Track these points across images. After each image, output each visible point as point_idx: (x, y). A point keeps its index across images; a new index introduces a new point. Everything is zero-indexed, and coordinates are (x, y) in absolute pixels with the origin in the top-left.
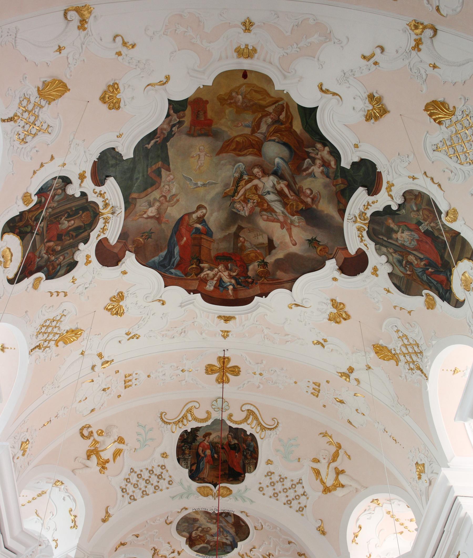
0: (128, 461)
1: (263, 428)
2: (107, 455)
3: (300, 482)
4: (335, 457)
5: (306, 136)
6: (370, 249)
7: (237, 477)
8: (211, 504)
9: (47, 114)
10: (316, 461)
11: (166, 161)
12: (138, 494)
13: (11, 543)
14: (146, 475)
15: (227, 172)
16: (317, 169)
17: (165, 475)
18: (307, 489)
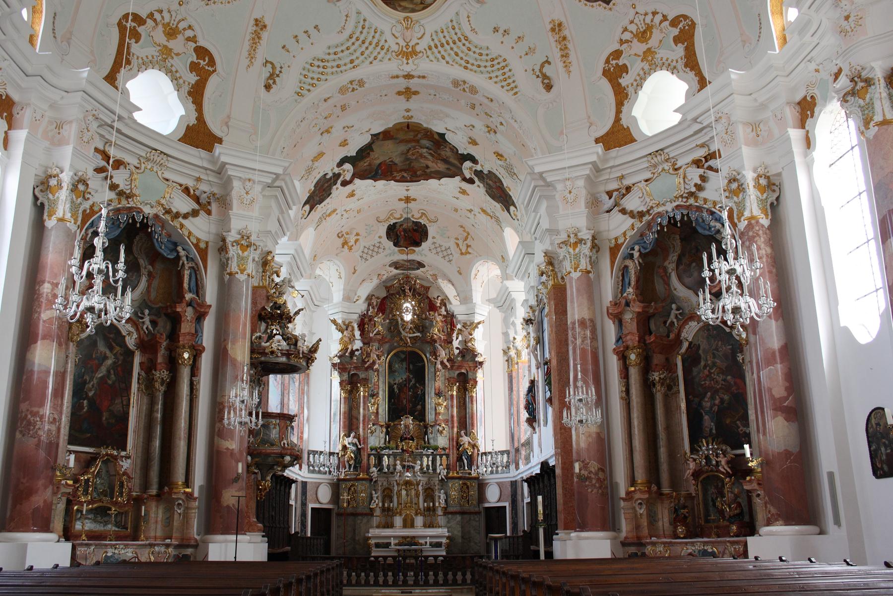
0: (362, 243)
1: (430, 222)
2: (352, 242)
3: (449, 248)
4: (466, 239)
5: (441, 140)
6: (476, 179)
7: (418, 244)
8: (404, 257)
9: (316, 164)
10: (457, 239)
14: (372, 248)
16: (447, 149)
17: (382, 246)
18: (453, 253)
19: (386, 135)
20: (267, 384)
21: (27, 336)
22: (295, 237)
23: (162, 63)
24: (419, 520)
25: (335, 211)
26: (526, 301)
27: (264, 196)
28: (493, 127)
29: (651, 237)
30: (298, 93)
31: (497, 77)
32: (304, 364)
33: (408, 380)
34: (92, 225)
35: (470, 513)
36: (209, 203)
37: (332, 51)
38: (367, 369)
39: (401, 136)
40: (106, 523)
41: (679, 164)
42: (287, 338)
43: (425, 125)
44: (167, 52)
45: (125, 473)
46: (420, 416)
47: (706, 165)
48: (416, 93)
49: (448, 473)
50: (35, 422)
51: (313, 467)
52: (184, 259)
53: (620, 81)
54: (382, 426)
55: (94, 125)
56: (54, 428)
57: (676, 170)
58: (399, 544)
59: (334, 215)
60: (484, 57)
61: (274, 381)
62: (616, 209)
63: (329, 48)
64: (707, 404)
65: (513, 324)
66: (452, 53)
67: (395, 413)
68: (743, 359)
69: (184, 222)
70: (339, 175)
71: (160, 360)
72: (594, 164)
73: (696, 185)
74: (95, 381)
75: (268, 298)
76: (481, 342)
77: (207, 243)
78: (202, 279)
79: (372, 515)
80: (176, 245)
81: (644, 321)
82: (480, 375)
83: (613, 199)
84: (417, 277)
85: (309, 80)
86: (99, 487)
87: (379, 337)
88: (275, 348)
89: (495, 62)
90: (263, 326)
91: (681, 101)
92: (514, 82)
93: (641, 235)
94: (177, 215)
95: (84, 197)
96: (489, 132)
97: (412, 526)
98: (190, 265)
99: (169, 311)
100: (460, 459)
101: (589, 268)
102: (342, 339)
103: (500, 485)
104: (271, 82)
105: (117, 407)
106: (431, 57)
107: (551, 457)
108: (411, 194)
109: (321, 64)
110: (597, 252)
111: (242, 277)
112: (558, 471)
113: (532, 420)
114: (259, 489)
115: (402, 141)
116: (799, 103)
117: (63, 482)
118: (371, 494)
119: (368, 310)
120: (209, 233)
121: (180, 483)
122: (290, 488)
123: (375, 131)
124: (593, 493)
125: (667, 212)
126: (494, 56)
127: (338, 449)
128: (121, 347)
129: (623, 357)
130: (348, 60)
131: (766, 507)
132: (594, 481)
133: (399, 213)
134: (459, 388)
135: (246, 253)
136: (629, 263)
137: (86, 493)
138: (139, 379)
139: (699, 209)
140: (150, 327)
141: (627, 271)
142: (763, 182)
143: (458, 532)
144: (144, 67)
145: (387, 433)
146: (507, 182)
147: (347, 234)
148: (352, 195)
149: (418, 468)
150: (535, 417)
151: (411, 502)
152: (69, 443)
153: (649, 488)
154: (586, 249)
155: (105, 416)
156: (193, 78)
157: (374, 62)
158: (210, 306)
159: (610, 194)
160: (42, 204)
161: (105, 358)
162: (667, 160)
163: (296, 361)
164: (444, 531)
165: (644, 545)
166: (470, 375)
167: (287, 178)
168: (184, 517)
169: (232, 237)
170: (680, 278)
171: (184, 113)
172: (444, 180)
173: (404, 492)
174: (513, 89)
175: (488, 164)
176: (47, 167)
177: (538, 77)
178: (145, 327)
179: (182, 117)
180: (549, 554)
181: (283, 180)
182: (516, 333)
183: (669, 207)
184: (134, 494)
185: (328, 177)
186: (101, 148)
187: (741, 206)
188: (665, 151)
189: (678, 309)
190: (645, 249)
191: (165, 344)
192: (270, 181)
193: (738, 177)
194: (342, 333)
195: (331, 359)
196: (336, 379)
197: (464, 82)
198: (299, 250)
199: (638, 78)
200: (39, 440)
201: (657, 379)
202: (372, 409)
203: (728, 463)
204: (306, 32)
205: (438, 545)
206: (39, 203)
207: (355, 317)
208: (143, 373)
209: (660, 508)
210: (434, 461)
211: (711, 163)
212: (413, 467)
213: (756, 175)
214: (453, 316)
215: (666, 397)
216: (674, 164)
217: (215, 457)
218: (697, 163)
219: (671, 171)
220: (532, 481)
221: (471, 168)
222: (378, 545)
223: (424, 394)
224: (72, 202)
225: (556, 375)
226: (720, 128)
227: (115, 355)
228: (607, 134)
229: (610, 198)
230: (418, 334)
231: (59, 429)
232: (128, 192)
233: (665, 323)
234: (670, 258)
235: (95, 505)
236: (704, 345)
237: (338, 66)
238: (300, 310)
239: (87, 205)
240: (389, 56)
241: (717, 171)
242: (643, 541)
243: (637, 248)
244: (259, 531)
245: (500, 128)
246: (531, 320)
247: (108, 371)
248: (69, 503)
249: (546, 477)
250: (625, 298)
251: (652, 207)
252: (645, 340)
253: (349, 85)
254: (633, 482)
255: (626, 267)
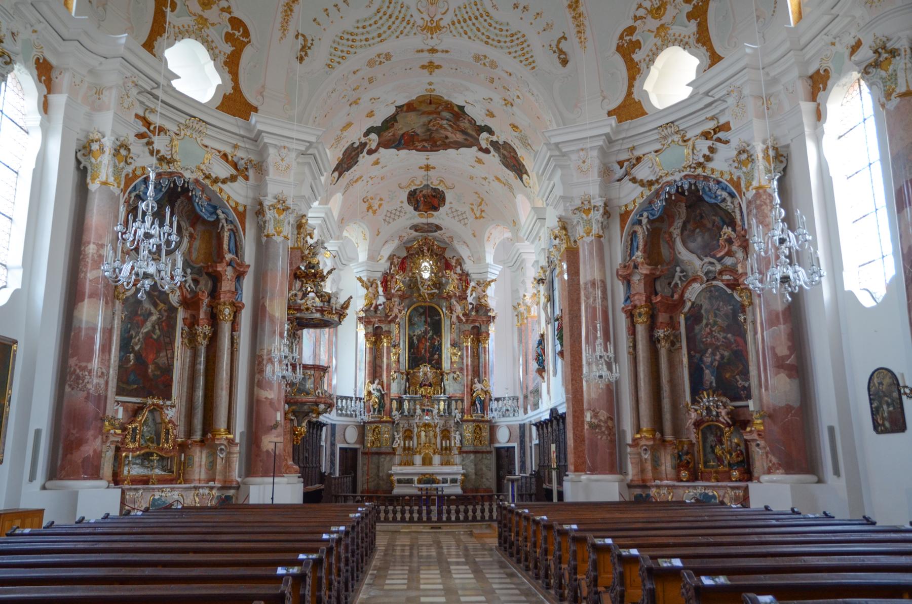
0: (386, 207)
2: (376, 207)
4: (480, 204)
6: (492, 149)
7: (436, 209)
8: (424, 221)
9: (345, 133)
11: (396, 121)
12: (391, 220)
13: (344, 262)
14: (394, 212)
15: (425, 119)
16: (466, 121)
19: (410, 107)
20: (300, 338)
21: (73, 294)
22: (325, 201)
23: (198, 32)
24: (436, 459)
25: (361, 177)
26: (537, 262)
27: (298, 163)
28: (510, 100)
29: (659, 204)
30: (328, 65)
31: (516, 52)
32: (336, 319)
33: (426, 332)
34: (135, 188)
35: (483, 452)
36: (247, 169)
37: (360, 25)
38: (390, 322)
39: (424, 108)
40: (152, 468)
41: (688, 136)
42: (320, 295)
43: (446, 98)
44: (203, 22)
45: (170, 422)
46: (437, 365)
47: (715, 137)
48: (438, 67)
49: (463, 416)
50: (84, 377)
51: (341, 410)
52: (224, 221)
53: (634, 56)
54: (402, 374)
55: (134, 91)
56: (102, 381)
57: (685, 141)
58: (420, 482)
59: (360, 182)
60: (504, 33)
61: (308, 335)
62: (627, 178)
63: (358, 22)
64: (708, 359)
65: (523, 282)
66: (474, 28)
67: (415, 361)
68: (745, 319)
69: (224, 187)
70: (365, 145)
71: (202, 315)
72: (607, 135)
73: (704, 156)
74: (141, 336)
75: (303, 258)
76: (493, 298)
77: (245, 207)
78: (241, 241)
79: (394, 454)
80: (215, 208)
81: (651, 282)
82: (492, 329)
83: (624, 169)
84: (435, 238)
85: (339, 53)
86: (146, 434)
87: (399, 293)
88: (310, 305)
89: (515, 38)
90: (298, 284)
91: (692, 76)
92: (532, 57)
93: (650, 203)
94: (216, 181)
95: (126, 161)
96: (506, 105)
97: (430, 464)
98: (229, 227)
99: (210, 270)
100: (473, 404)
101: (601, 233)
102: (367, 295)
103: (509, 427)
104: (303, 54)
105: (162, 360)
106: (454, 33)
107: (561, 404)
108: (431, 162)
109: (351, 38)
110: (608, 218)
111: (279, 239)
112: (569, 420)
113: (541, 370)
114: (294, 434)
115: (424, 113)
116: (811, 77)
117: (112, 431)
118: (394, 435)
119: (390, 269)
120: (247, 197)
121: (222, 430)
122: (321, 431)
123: (399, 103)
124: (603, 440)
125: (675, 181)
126: (513, 32)
127: (363, 394)
128: (165, 303)
129: (631, 315)
130: (375, 34)
131: (767, 457)
132: (603, 429)
133: (419, 180)
134: (473, 340)
135: (282, 217)
136: (638, 228)
137: (134, 440)
138: (182, 334)
139: (706, 178)
140: (192, 285)
141: (636, 236)
142: (771, 153)
143: (471, 470)
144: (181, 36)
145: (408, 380)
146: (521, 153)
147: (372, 199)
148: (377, 163)
149: (435, 411)
150: (544, 368)
151: (430, 443)
152: (117, 394)
153: (654, 435)
154: (597, 216)
155: (151, 368)
156: (228, 49)
157: (401, 36)
158: (249, 266)
159: (621, 164)
160: (85, 168)
161: (150, 314)
162: (677, 133)
163: (329, 316)
164: (458, 469)
165: (649, 487)
166: (483, 329)
167: (320, 147)
168: (226, 461)
169: (268, 201)
170: (684, 243)
171: (220, 82)
172: (462, 150)
173: (423, 434)
174: (531, 63)
175: (503, 135)
176: (88, 132)
177: (555, 52)
178: (187, 285)
179: (219, 86)
180: (561, 495)
181: (316, 148)
182: (526, 290)
183: (677, 177)
184: (179, 440)
185: (355, 146)
186: (142, 115)
187: (750, 177)
188: (676, 123)
189: (682, 272)
190: (653, 215)
191: (206, 300)
192: (303, 149)
193: (748, 148)
194: (367, 289)
195: (357, 313)
196: (362, 331)
197: (485, 57)
198: (329, 213)
199: (650, 54)
200: (88, 393)
201: (662, 335)
202: (393, 358)
203: (728, 414)
204: (336, 6)
205: (454, 481)
206: (81, 166)
207: (379, 275)
208: (186, 328)
209: (663, 454)
210: (449, 405)
211: (720, 135)
212: (432, 411)
213: (765, 147)
214: (467, 275)
215: (670, 352)
216: (683, 136)
217: (254, 407)
218: (706, 135)
219: (680, 143)
220: (540, 425)
221: (487, 139)
222: (399, 481)
223: (440, 345)
224: (115, 166)
225: (568, 330)
226: (731, 101)
227: (160, 311)
228: (619, 107)
229: (621, 168)
230: (436, 291)
231: (107, 383)
232: (169, 157)
233: (669, 284)
234: (675, 224)
235: (142, 452)
236: (706, 305)
237: (367, 40)
238: (332, 270)
239: (129, 169)
240: (414, 30)
241: (727, 142)
242: (648, 484)
243: (645, 214)
244: (296, 472)
245: (517, 101)
246: (542, 279)
247: (153, 327)
248: (118, 449)
249: (555, 422)
250: (634, 261)
251: (661, 177)
252: (651, 300)
253: (377, 59)
254: (638, 430)
255: (635, 232)
